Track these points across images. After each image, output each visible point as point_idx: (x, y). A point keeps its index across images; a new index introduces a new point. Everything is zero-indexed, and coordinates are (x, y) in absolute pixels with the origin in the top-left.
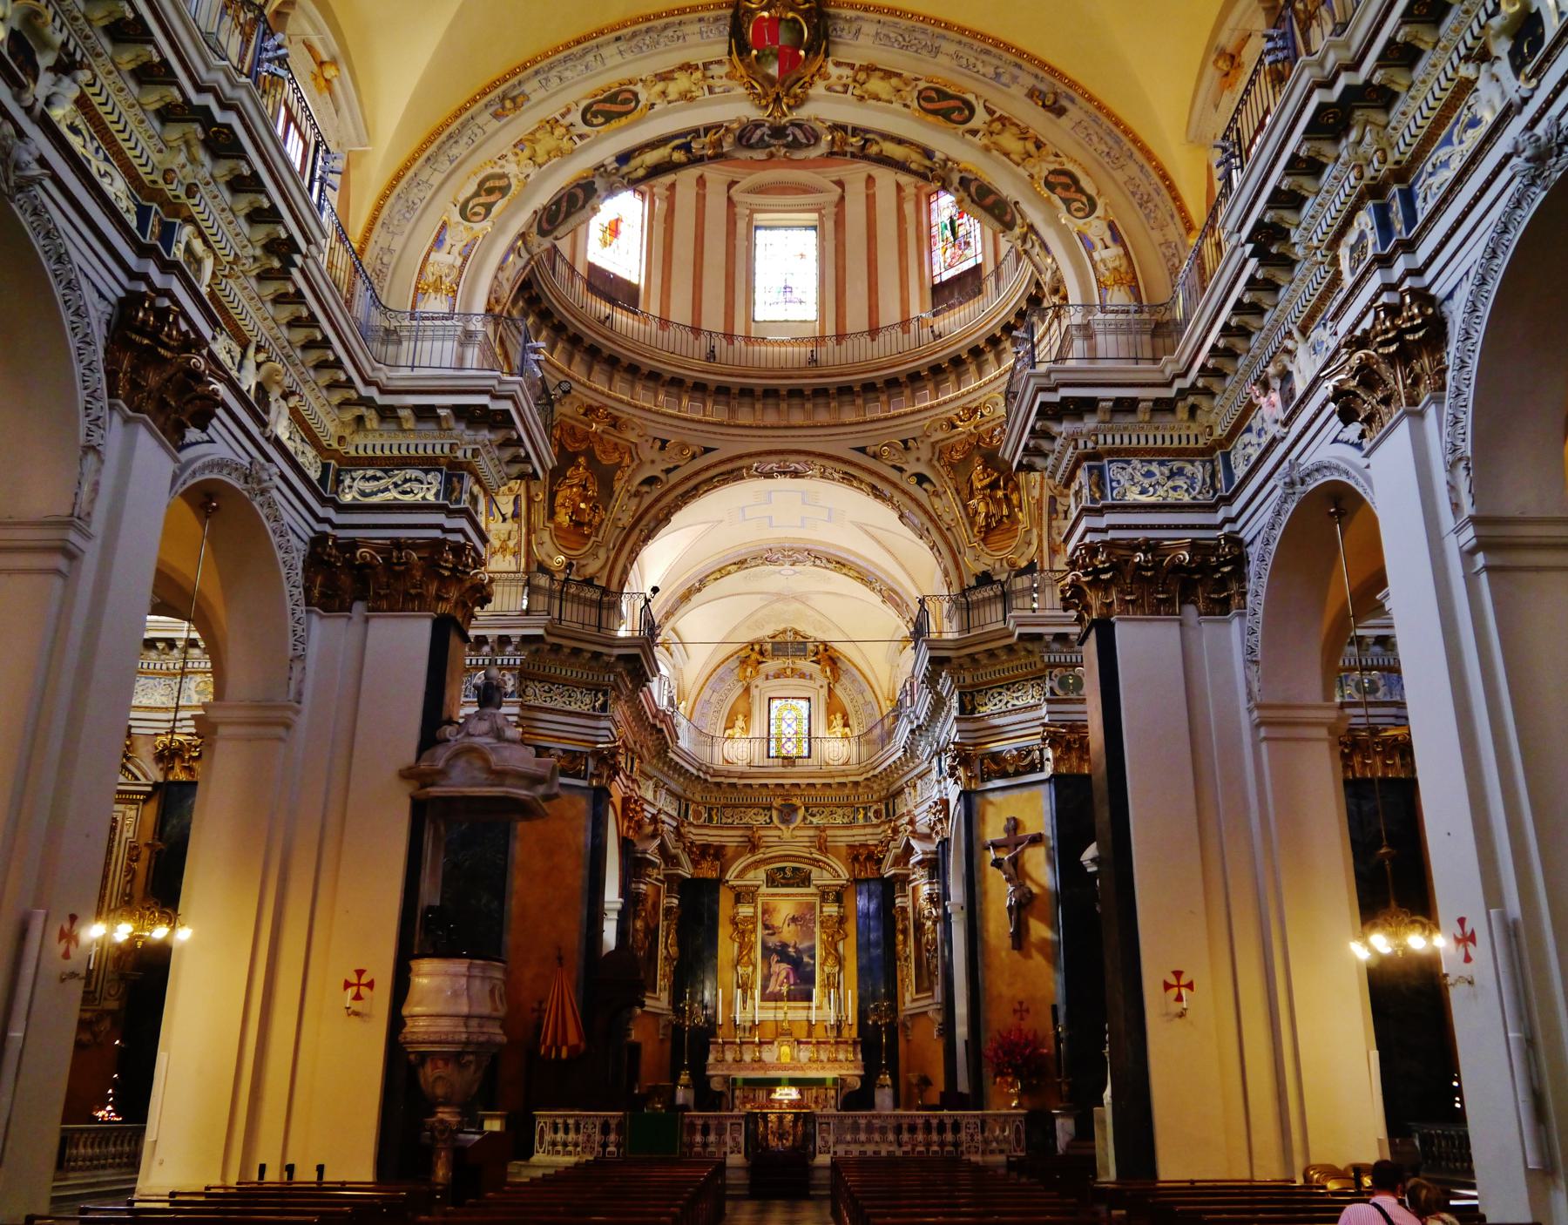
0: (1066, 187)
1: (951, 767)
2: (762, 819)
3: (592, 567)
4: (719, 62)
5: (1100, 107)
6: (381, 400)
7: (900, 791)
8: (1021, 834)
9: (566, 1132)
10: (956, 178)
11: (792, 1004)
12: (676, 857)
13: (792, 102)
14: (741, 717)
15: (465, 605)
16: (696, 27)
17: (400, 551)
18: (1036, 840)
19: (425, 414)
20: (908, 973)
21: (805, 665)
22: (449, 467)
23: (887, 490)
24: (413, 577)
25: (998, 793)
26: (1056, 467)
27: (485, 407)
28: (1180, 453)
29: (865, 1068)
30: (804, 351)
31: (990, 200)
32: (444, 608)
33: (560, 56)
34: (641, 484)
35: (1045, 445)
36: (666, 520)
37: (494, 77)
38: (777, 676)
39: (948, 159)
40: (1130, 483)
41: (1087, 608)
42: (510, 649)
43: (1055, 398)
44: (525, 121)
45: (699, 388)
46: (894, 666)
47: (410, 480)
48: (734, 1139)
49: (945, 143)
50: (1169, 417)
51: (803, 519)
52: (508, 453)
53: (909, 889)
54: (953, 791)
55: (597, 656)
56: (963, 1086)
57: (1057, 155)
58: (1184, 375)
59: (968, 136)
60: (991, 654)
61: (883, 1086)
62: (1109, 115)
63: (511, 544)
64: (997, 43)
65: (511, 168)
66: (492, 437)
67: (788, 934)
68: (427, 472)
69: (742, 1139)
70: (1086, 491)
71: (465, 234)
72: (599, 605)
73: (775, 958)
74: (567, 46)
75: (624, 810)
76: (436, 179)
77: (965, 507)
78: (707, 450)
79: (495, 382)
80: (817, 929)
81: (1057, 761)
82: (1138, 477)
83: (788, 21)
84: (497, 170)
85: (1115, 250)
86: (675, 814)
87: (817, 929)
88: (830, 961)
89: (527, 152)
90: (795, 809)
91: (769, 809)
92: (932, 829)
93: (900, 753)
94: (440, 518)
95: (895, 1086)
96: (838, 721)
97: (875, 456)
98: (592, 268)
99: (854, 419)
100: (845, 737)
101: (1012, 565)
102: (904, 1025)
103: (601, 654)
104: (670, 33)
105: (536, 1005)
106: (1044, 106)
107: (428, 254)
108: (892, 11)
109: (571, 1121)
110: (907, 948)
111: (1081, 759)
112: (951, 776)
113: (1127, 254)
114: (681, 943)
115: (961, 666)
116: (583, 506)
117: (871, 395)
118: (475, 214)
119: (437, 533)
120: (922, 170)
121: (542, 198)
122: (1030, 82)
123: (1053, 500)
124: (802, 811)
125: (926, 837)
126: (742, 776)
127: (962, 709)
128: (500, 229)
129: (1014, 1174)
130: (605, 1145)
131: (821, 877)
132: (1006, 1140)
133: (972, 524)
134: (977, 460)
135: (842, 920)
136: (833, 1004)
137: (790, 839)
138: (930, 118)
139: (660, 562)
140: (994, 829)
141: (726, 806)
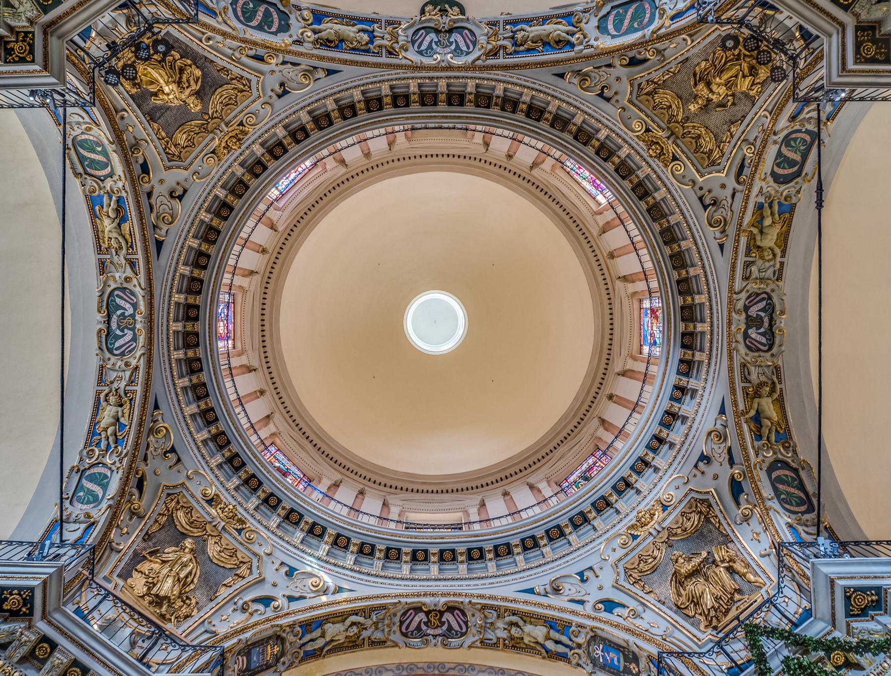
34: (254, 601)
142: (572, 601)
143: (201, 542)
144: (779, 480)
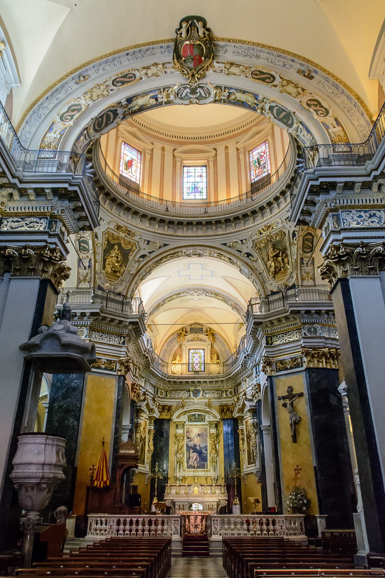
0: (316, 106)
1: (263, 367)
2: (186, 395)
3: (120, 289)
4: (170, 63)
5: (329, 74)
6: (20, 186)
7: (240, 384)
8: (294, 393)
9: (101, 524)
10: (267, 107)
11: (199, 470)
12: (152, 409)
13: (199, 77)
14: (178, 356)
15: (55, 276)
16: (160, 50)
17: (26, 250)
18: (301, 395)
19: (39, 193)
20: (244, 457)
21: (202, 336)
22: (50, 217)
23: (235, 260)
24: (31, 261)
25: (284, 376)
26: (315, 220)
27: (66, 189)
28: (373, 207)
29: (229, 497)
30: (202, 210)
31: (283, 114)
32: (45, 276)
33: (104, 60)
34: (140, 257)
35: (311, 209)
36: (149, 272)
37: (76, 67)
38: (192, 340)
39: (264, 98)
40: (351, 220)
41: (335, 275)
42: (86, 318)
43: (317, 183)
44: (89, 85)
45: (162, 221)
46: (236, 336)
47: (33, 222)
48: (175, 527)
49: (263, 90)
50: (368, 191)
51: (202, 276)
52: (77, 216)
53: (244, 422)
54: (263, 379)
55: (121, 322)
56: (271, 503)
57: (311, 94)
58: (377, 169)
59: (273, 87)
60: (279, 320)
61: (236, 504)
62: (333, 76)
63: (88, 278)
64: (284, 52)
65: (83, 102)
66: (70, 204)
67: (197, 441)
68: (40, 219)
69: (179, 528)
70: (331, 225)
71: (62, 126)
72: (122, 303)
73: (191, 451)
74: (106, 56)
75: (132, 389)
76: (51, 106)
77: (266, 265)
78: (165, 245)
79: (70, 178)
80: (208, 439)
81: (309, 361)
82: (355, 218)
83: (197, 45)
84: (76, 103)
85: (338, 128)
86: (153, 393)
87: (208, 439)
88: (214, 451)
89: (89, 95)
90: (199, 391)
91: (189, 391)
92: (253, 396)
93: (240, 367)
94: (46, 237)
95: (241, 504)
96: (215, 357)
97: (230, 247)
98: (121, 175)
99: (222, 233)
100: (218, 363)
101: (286, 286)
102: (243, 478)
103: (123, 321)
104: (149, 52)
105: (92, 467)
106: (304, 76)
107: (46, 134)
108: (240, 41)
109: (103, 519)
110: (244, 446)
111: (318, 361)
112: (263, 371)
113: (343, 130)
114: (155, 445)
115: (266, 325)
116: (116, 264)
117: (228, 224)
118: (67, 119)
119: (44, 244)
120: (253, 106)
121: (95, 114)
122: (299, 67)
123: (302, 259)
124: (201, 392)
125: (251, 400)
126: (179, 378)
127: (267, 343)
128: (76, 124)
129: (312, 547)
130: (118, 531)
131: (209, 418)
132: (296, 529)
133: (269, 271)
134: (270, 246)
135: (218, 436)
136: (215, 469)
137: (198, 402)
138: (257, 81)
139: (148, 291)
140: (281, 391)
141: (172, 390)
143: (119, 245)
144: (307, 240)
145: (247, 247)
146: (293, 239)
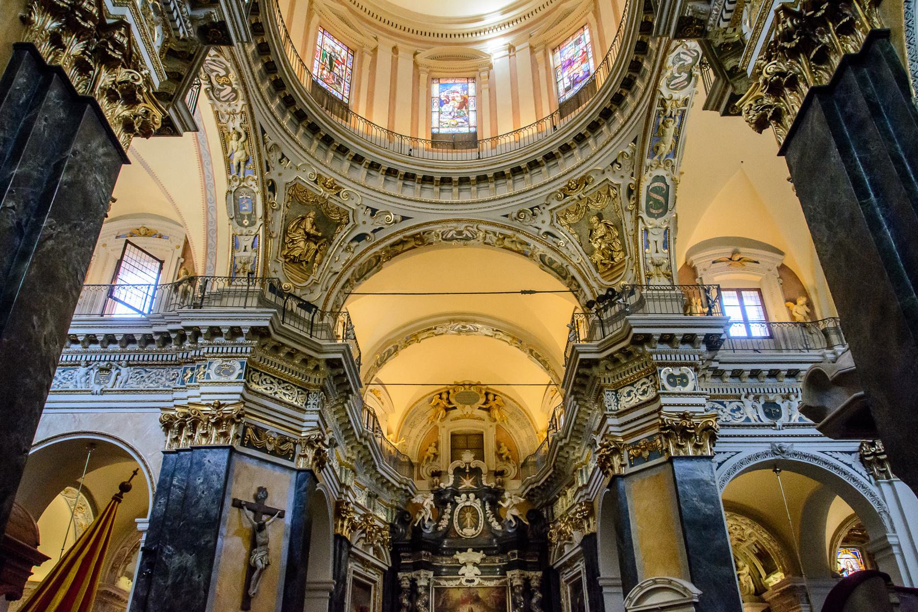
8: (268, 503)
25: (255, 462)
140: (243, 490)
142: (267, 162)
145: (280, 174)
146: (352, 241)
